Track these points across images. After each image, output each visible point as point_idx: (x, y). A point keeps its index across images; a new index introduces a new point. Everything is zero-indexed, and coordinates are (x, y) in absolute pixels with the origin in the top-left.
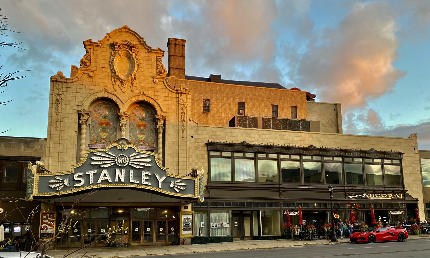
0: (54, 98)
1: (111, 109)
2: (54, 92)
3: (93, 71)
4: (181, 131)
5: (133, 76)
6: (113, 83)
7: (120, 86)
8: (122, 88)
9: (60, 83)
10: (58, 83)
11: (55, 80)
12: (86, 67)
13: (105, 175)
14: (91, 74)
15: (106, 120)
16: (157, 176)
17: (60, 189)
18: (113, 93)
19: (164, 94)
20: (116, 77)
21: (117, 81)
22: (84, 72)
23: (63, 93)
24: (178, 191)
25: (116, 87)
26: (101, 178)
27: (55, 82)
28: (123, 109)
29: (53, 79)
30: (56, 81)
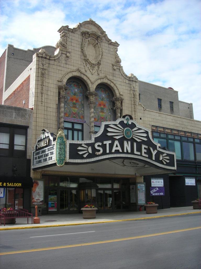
0: (39, 72)
1: (79, 88)
2: (40, 66)
3: (69, 53)
5: (99, 61)
6: (85, 65)
7: (89, 67)
8: (91, 70)
9: (45, 59)
10: (43, 59)
11: (41, 56)
12: (64, 48)
13: (117, 146)
14: (68, 54)
15: (76, 96)
16: (151, 149)
17: (85, 156)
18: (85, 73)
19: (120, 80)
20: (86, 60)
22: (63, 52)
23: (47, 68)
24: (165, 163)
25: (87, 69)
26: (114, 149)
27: (40, 58)
28: (92, 88)
29: (39, 55)
30: (42, 57)
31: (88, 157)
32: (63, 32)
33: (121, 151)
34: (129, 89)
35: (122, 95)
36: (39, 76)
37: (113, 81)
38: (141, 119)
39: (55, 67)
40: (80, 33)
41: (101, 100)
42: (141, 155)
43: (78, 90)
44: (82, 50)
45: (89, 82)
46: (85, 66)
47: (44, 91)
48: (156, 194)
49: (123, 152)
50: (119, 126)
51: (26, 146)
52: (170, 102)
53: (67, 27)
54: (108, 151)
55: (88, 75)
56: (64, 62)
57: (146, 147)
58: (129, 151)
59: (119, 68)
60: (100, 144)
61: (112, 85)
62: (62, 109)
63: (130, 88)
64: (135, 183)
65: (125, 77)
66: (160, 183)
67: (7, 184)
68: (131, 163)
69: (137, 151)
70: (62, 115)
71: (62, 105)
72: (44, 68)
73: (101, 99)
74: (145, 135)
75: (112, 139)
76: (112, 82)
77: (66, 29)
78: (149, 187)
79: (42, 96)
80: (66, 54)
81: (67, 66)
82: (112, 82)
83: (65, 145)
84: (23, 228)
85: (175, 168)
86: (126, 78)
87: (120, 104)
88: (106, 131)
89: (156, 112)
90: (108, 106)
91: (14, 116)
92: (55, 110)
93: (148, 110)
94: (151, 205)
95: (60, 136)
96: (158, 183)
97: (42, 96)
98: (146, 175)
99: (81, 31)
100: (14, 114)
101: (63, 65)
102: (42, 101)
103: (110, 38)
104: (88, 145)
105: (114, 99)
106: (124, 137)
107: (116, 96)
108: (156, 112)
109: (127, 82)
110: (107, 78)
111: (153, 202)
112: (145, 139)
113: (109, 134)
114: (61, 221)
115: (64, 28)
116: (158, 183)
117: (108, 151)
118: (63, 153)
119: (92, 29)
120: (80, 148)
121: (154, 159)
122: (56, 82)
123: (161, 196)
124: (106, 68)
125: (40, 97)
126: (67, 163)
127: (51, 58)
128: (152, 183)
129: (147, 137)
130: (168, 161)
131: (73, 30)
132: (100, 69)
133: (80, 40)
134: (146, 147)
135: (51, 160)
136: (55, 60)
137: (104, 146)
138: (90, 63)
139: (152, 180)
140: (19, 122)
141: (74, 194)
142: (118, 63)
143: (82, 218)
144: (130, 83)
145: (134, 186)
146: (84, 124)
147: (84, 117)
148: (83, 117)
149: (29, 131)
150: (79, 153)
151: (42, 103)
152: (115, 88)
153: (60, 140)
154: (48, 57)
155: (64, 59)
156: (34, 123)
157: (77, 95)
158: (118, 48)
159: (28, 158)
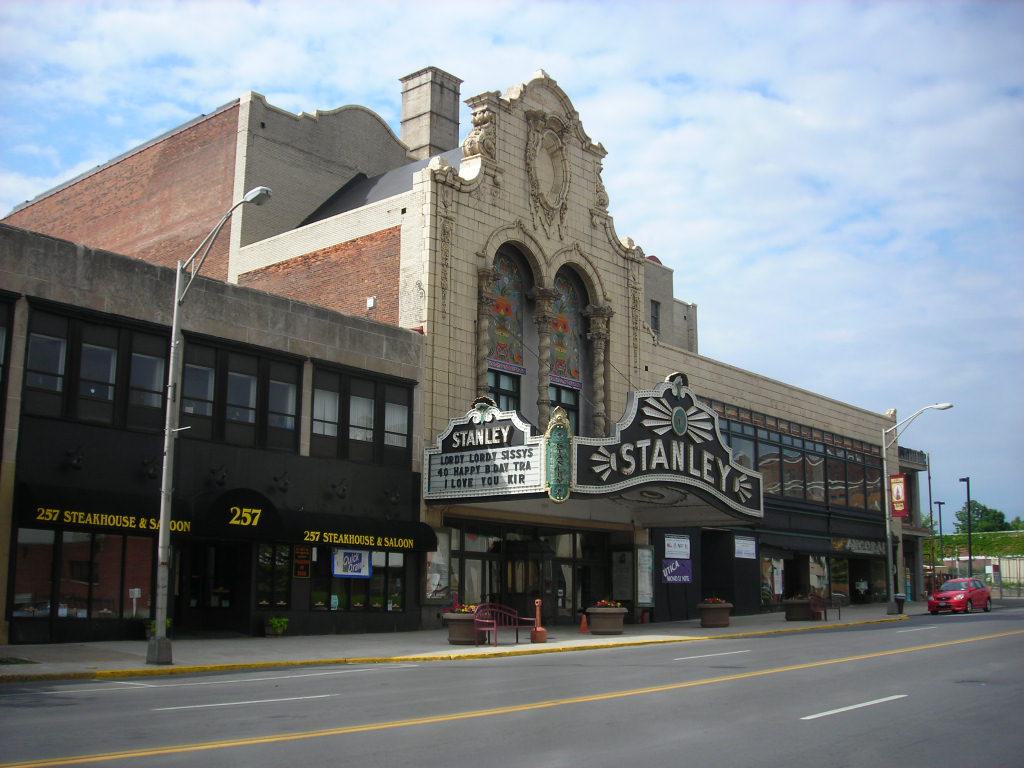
4: (632, 350)
6: (533, 210)
8: (546, 226)
9: (450, 190)
10: (446, 188)
13: (660, 455)
16: (720, 463)
17: (605, 477)
19: (606, 256)
20: (536, 197)
21: (540, 209)
22: (488, 171)
25: (537, 222)
26: (656, 461)
27: (440, 185)
28: (549, 275)
29: (438, 177)
30: (444, 183)
31: (610, 481)
32: (487, 109)
33: (666, 466)
34: (624, 282)
35: (610, 301)
36: (438, 237)
37: (591, 258)
39: (470, 213)
40: (521, 114)
41: (499, 294)
42: (701, 479)
44: (527, 164)
45: (541, 261)
46: (534, 212)
48: (675, 579)
49: (670, 471)
50: (664, 401)
51: (409, 436)
52: (652, 301)
53: (498, 94)
54: (644, 468)
55: (537, 238)
56: (488, 198)
57: (711, 457)
58: (681, 468)
59: (603, 221)
60: (631, 447)
61: (589, 270)
62: (486, 337)
64: (631, 548)
65: (617, 248)
66: (681, 549)
67: (383, 542)
68: (645, 494)
69: (695, 467)
70: (486, 351)
71: (486, 323)
72: (450, 215)
74: (708, 427)
75: (649, 433)
76: (589, 261)
77: (495, 100)
78: (660, 560)
79: (444, 297)
80: (494, 177)
81: (496, 212)
82: (589, 261)
83: (570, 448)
84: (559, 651)
85: (760, 513)
86: (620, 251)
87: (604, 326)
88: (641, 415)
89: (679, 349)
90: (573, 329)
91: (384, 350)
92: (470, 339)
93: (663, 344)
94: (714, 606)
95: (560, 426)
96: (678, 549)
97: (444, 297)
98: (655, 526)
99: (526, 109)
100: (385, 343)
101: (486, 208)
102: (444, 312)
103: (588, 132)
104: (610, 448)
105: (589, 309)
106: (672, 431)
107: (596, 302)
108: (679, 349)
109: (621, 262)
111: (722, 598)
112: (709, 438)
113: (647, 423)
114: (634, 634)
115: (491, 98)
116: (678, 548)
117: (644, 468)
118: (567, 468)
119: (550, 108)
120: (596, 458)
121: (724, 489)
122: (472, 258)
123: (683, 584)
124: (577, 219)
126: (574, 495)
127: (464, 188)
128: (667, 549)
129: (713, 432)
130: (749, 496)
131: (509, 105)
132: (565, 224)
133: (522, 135)
134: (711, 457)
135: (522, 484)
136: (469, 192)
137: (636, 453)
138: (545, 206)
139: (668, 541)
140: (395, 367)
141: (554, 572)
142: (601, 207)
143: (446, 644)
145: (628, 555)
146: (523, 379)
148: (521, 357)
149: (418, 394)
150: (595, 468)
151: (444, 318)
152: (595, 280)
153: (560, 435)
154: (458, 184)
155: (488, 191)
156: (427, 373)
157: (509, 294)
158: (603, 161)
159: (414, 469)
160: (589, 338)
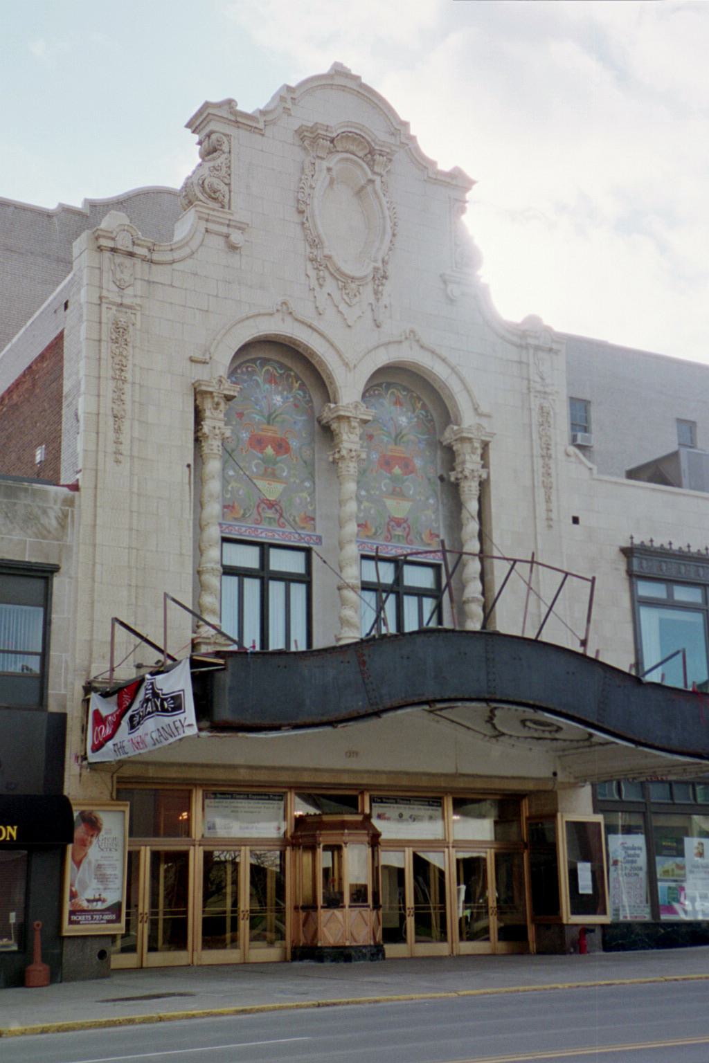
0: (104, 320)
1: (291, 388)
2: (105, 293)
3: (241, 228)
4: (540, 493)
5: (379, 264)
6: (314, 283)
7: (337, 295)
8: (342, 307)
9: (128, 262)
10: (119, 259)
11: (111, 244)
12: (216, 206)
14: (236, 237)
18: (315, 323)
20: (321, 263)
21: (329, 279)
22: (211, 226)
23: (138, 301)
27: (107, 254)
28: (349, 388)
30: (113, 250)
36: (104, 338)
38: (576, 520)
43: (285, 399)
46: (317, 288)
47: (128, 406)
51: (44, 655)
61: (440, 371)
62: (214, 486)
63: (526, 382)
68: (528, 724)
72: (127, 301)
73: (263, 416)
79: (118, 430)
80: (227, 236)
97: (118, 430)
102: (118, 453)
110: (418, 341)
125: (111, 435)
132: (385, 300)
144: (524, 359)
147: (313, 519)
159: (53, 707)
160: (453, 479)
